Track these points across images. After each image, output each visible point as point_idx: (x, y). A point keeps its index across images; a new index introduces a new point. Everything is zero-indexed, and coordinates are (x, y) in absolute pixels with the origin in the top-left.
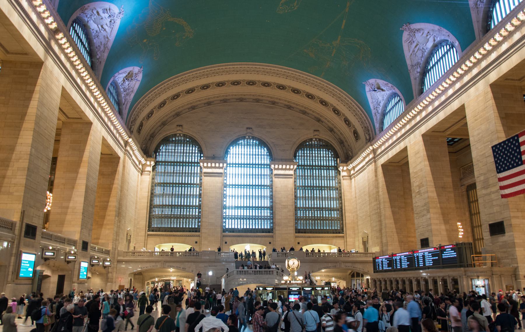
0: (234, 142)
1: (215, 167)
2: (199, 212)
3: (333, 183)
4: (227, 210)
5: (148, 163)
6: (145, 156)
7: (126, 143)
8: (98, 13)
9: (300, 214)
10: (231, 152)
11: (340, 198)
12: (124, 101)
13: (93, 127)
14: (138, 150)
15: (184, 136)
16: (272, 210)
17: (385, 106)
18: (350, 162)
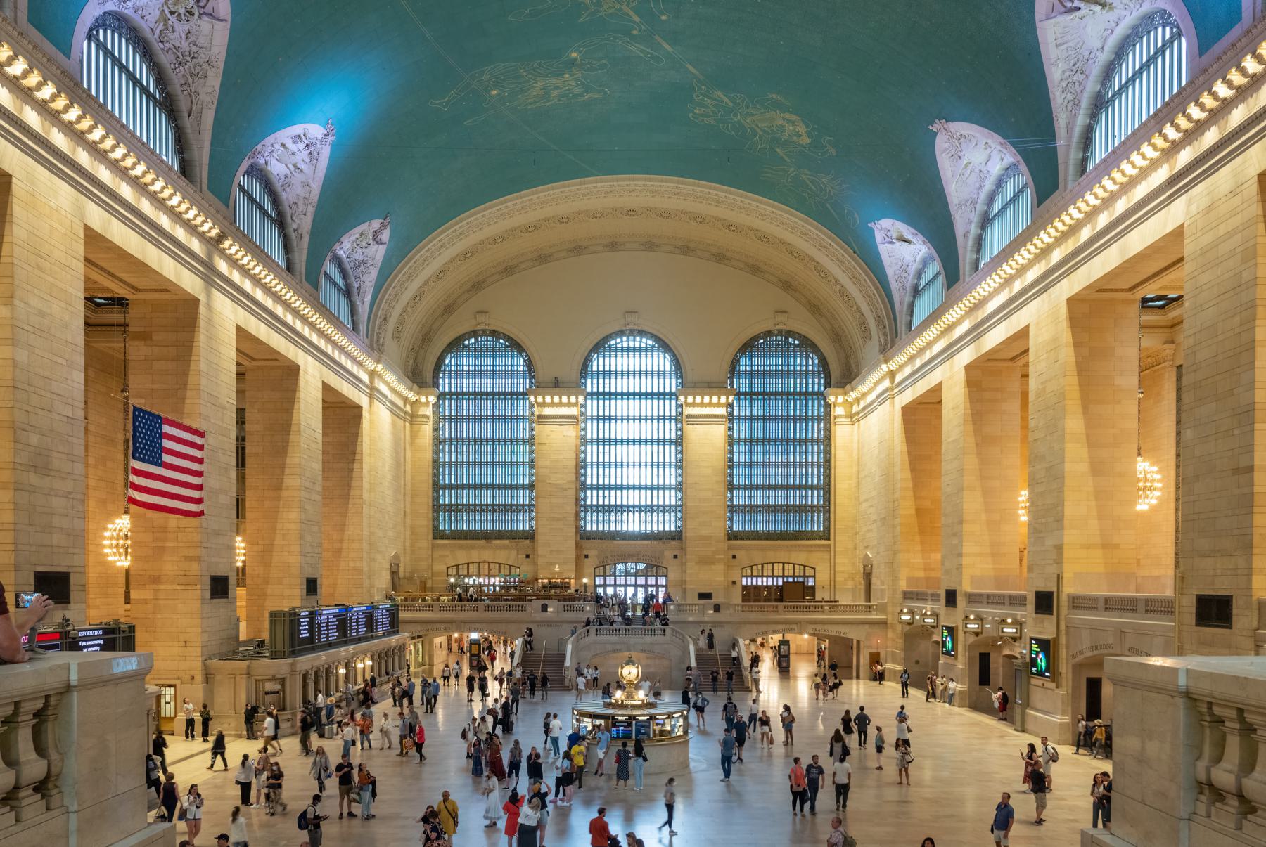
0: (600, 346)
1: (560, 404)
2: (531, 499)
3: (816, 431)
4: (589, 492)
5: (423, 399)
6: (415, 387)
7: (372, 374)
8: (283, 145)
9: (740, 498)
10: (595, 369)
11: (827, 464)
12: (356, 285)
13: (301, 372)
14: (400, 379)
15: (495, 334)
16: (681, 491)
17: (919, 274)
18: (848, 387)
